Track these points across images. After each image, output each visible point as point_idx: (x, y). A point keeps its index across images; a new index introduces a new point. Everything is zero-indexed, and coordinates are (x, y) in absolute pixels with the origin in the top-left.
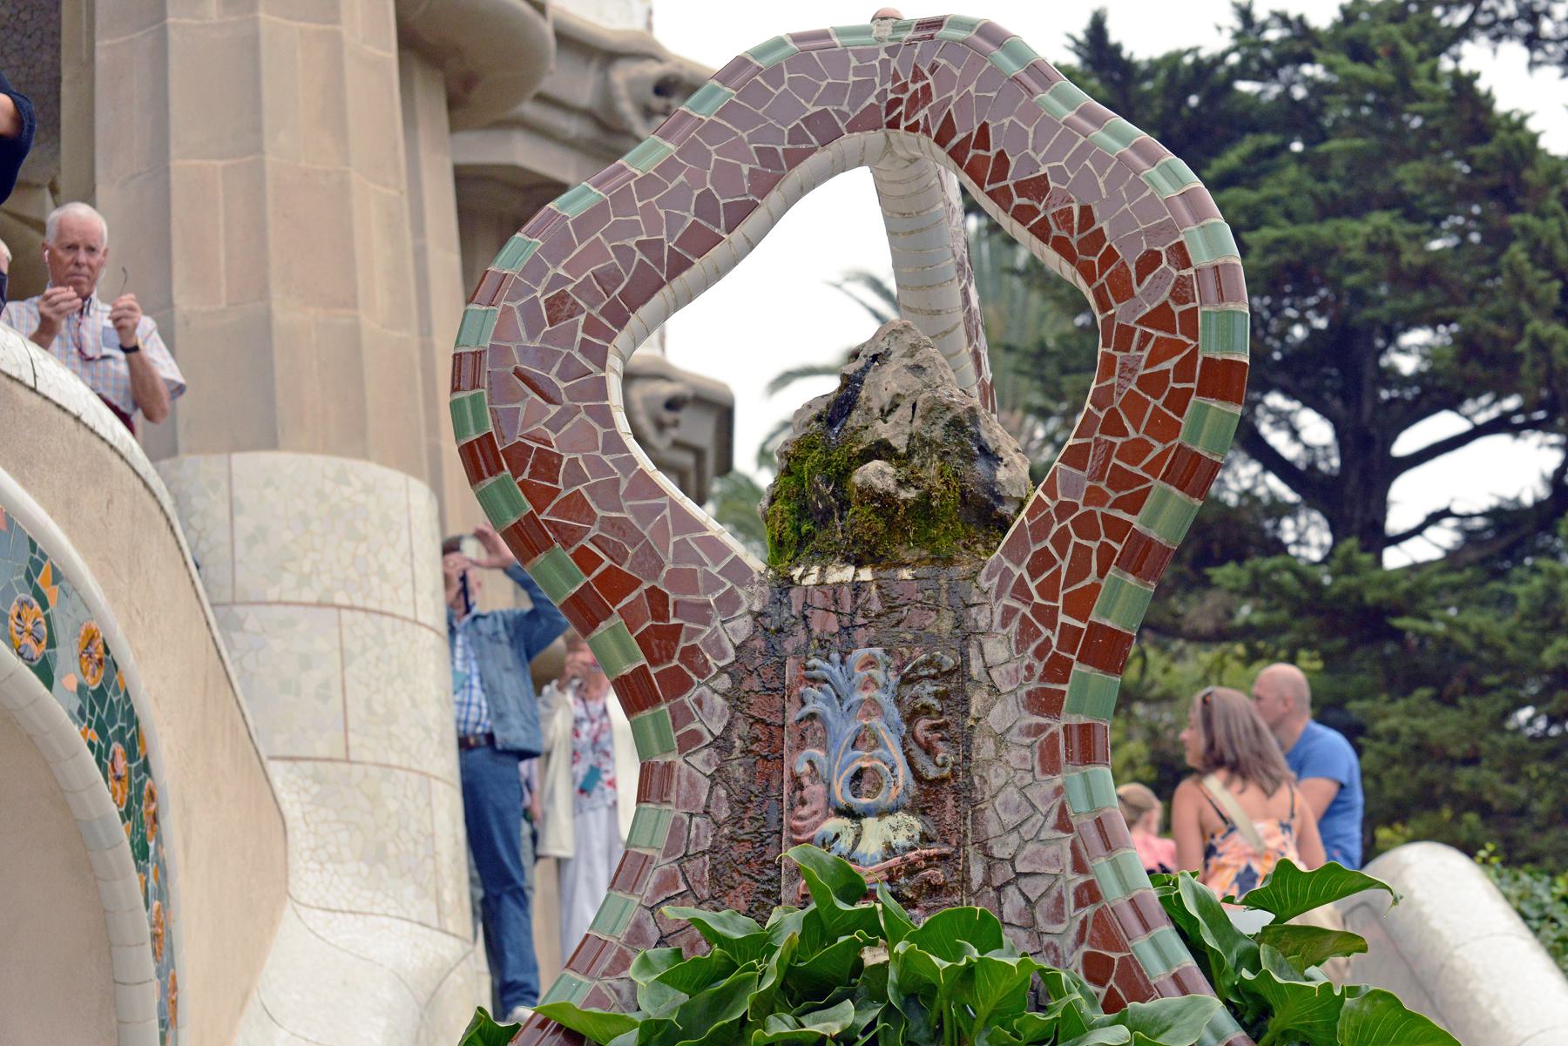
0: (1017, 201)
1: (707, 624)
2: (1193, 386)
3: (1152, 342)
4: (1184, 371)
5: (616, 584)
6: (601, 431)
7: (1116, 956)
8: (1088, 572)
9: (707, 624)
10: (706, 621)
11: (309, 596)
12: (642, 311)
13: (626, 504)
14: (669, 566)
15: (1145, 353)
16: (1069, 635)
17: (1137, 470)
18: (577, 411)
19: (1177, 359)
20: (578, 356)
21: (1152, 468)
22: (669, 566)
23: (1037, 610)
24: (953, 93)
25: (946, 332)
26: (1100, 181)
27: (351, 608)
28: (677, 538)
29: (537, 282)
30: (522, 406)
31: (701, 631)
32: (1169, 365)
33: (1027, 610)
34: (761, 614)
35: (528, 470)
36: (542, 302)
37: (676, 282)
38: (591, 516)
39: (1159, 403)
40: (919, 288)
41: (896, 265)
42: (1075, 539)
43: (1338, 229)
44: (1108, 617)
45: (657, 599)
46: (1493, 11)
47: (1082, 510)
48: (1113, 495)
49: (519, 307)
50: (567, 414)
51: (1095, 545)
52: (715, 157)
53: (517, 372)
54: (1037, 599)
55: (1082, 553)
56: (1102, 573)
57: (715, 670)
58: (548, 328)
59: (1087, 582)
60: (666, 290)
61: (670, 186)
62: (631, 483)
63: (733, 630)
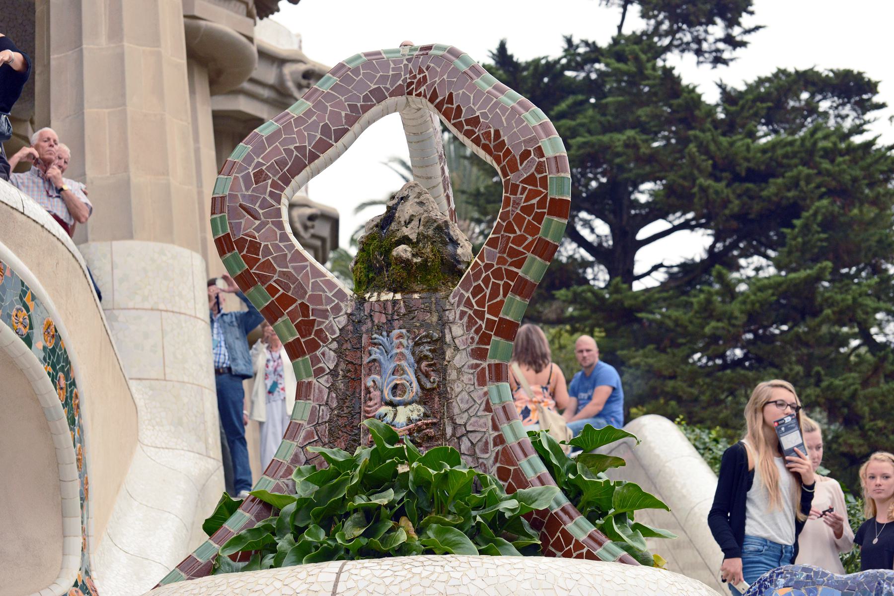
0: (466, 128)
1: (327, 319)
2: (546, 211)
3: (527, 191)
4: (541, 204)
5: (286, 301)
6: (278, 232)
7: (512, 468)
8: (499, 295)
9: (327, 319)
10: (327, 318)
11: (147, 305)
12: (297, 178)
13: (290, 265)
14: (309, 293)
15: (524, 196)
16: (490, 323)
17: (521, 249)
18: (268, 223)
19: (538, 199)
20: (268, 198)
21: (527, 248)
22: (309, 293)
23: (476, 312)
24: (437, 79)
25: (434, 187)
26: (503, 118)
27: (167, 311)
28: (313, 280)
29: (250, 165)
30: (243, 221)
31: (324, 322)
32: (534, 201)
33: (471, 312)
34: (351, 314)
35: (246, 250)
36: (252, 174)
37: (312, 165)
38: (274, 271)
39: (530, 218)
40: (422, 167)
41: (411, 157)
42: (493, 280)
43: (611, 138)
44: (507, 315)
45: (304, 308)
46: (680, 39)
47: (496, 267)
48: (510, 260)
49: (242, 177)
50: (263, 225)
51: (502, 283)
52: (329, 108)
53: (241, 206)
54: (476, 307)
55: (496, 287)
56: (505, 295)
57: (330, 340)
58: (254, 186)
59: (498, 299)
60: (307, 168)
61: (309, 122)
62: (292, 255)
63: (338, 321)
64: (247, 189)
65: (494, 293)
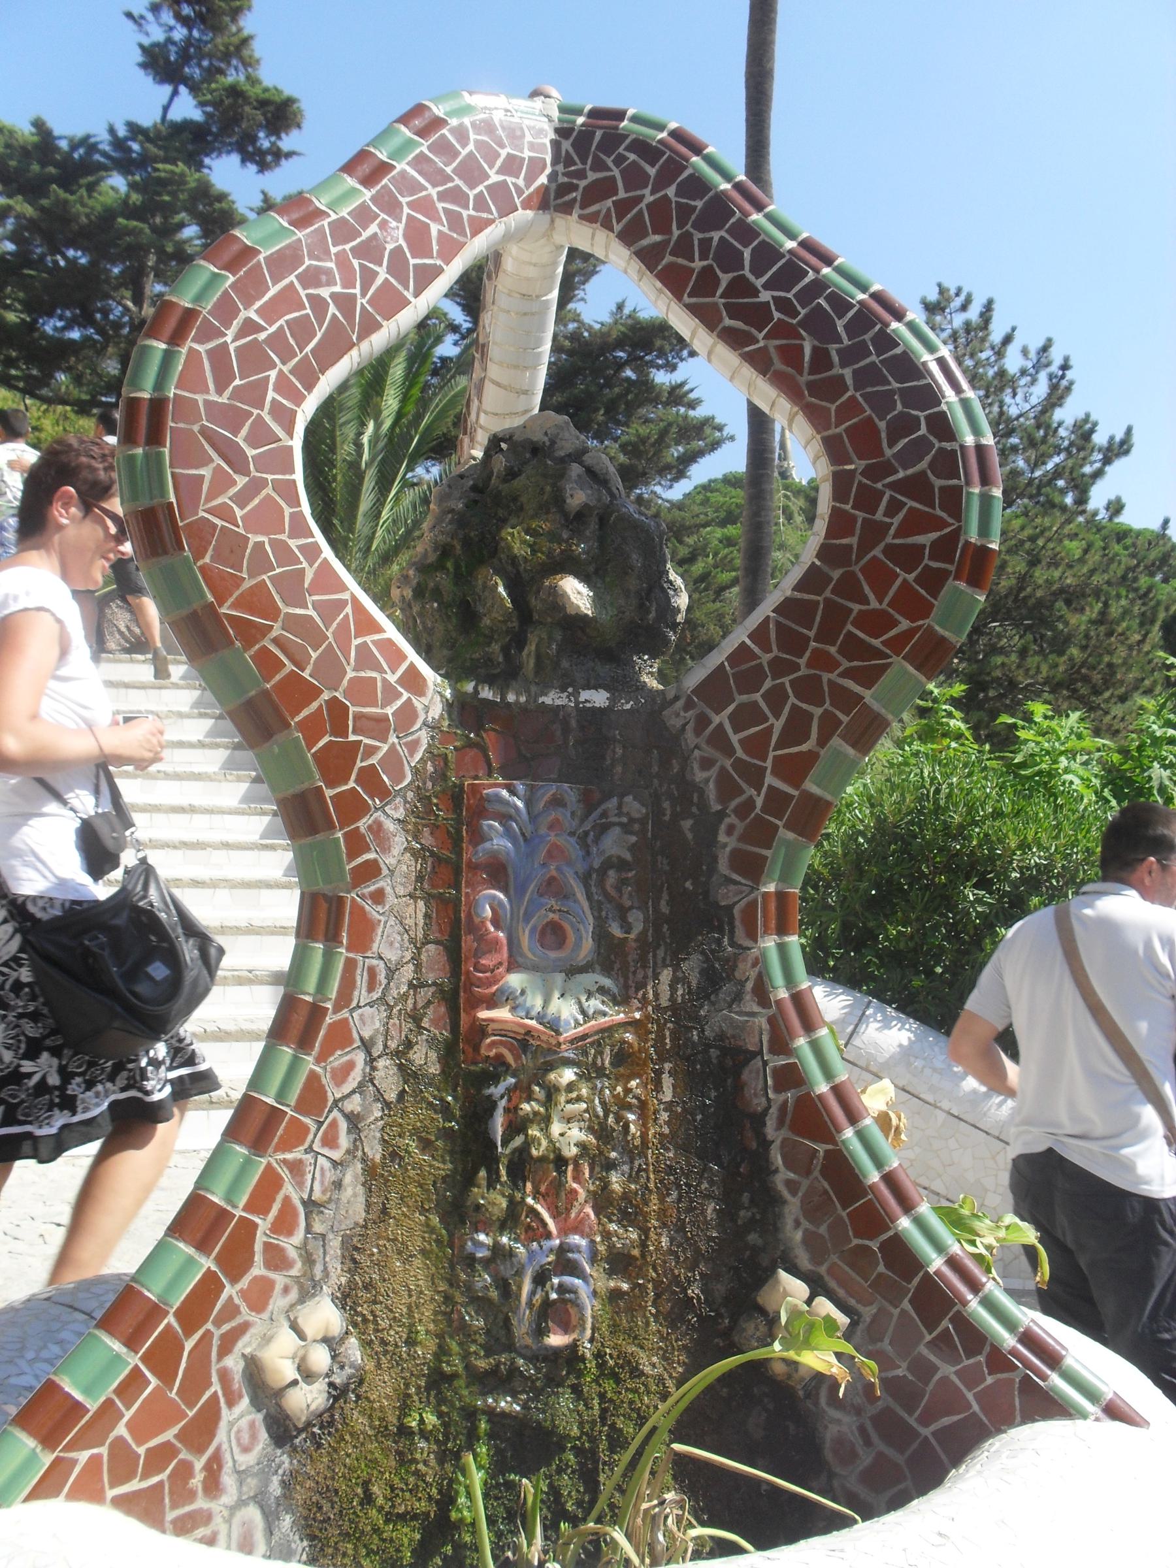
3: (905, 511)
8: (806, 737)
9: (384, 740)
16: (776, 801)
19: (934, 535)
20: (268, 419)
22: (350, 674)
28: (359, 641)
29: (228, 324)
32: (926, 539)
35: (210, 553)
36: (232, 348)
39: (911, 577)
42: (792, 699)
45: (337, 709)
48: (846, 664)
49: (208, 352)
53: (204, 431)
58: (237, 382)
59: (804, 747)
62: (317, 573)
64: (220, 392)
65: (796, 729)
